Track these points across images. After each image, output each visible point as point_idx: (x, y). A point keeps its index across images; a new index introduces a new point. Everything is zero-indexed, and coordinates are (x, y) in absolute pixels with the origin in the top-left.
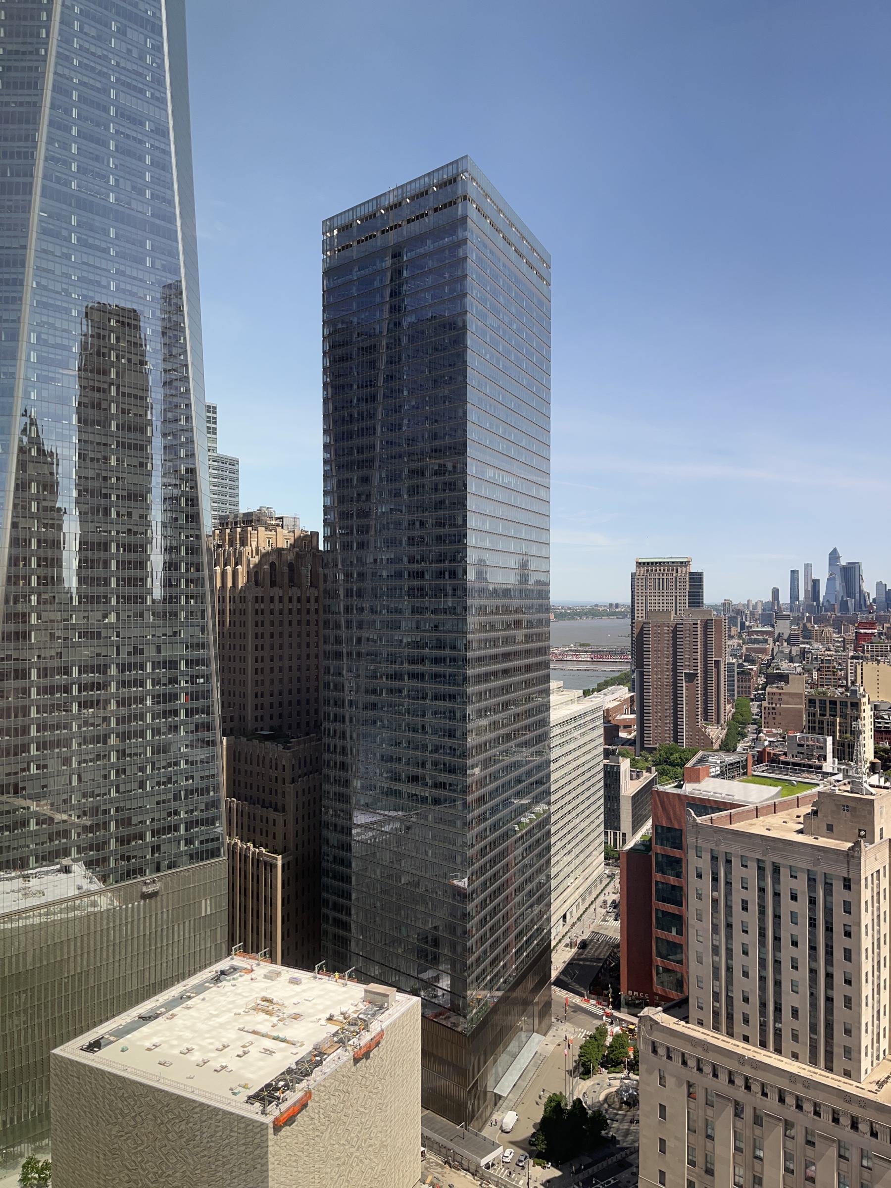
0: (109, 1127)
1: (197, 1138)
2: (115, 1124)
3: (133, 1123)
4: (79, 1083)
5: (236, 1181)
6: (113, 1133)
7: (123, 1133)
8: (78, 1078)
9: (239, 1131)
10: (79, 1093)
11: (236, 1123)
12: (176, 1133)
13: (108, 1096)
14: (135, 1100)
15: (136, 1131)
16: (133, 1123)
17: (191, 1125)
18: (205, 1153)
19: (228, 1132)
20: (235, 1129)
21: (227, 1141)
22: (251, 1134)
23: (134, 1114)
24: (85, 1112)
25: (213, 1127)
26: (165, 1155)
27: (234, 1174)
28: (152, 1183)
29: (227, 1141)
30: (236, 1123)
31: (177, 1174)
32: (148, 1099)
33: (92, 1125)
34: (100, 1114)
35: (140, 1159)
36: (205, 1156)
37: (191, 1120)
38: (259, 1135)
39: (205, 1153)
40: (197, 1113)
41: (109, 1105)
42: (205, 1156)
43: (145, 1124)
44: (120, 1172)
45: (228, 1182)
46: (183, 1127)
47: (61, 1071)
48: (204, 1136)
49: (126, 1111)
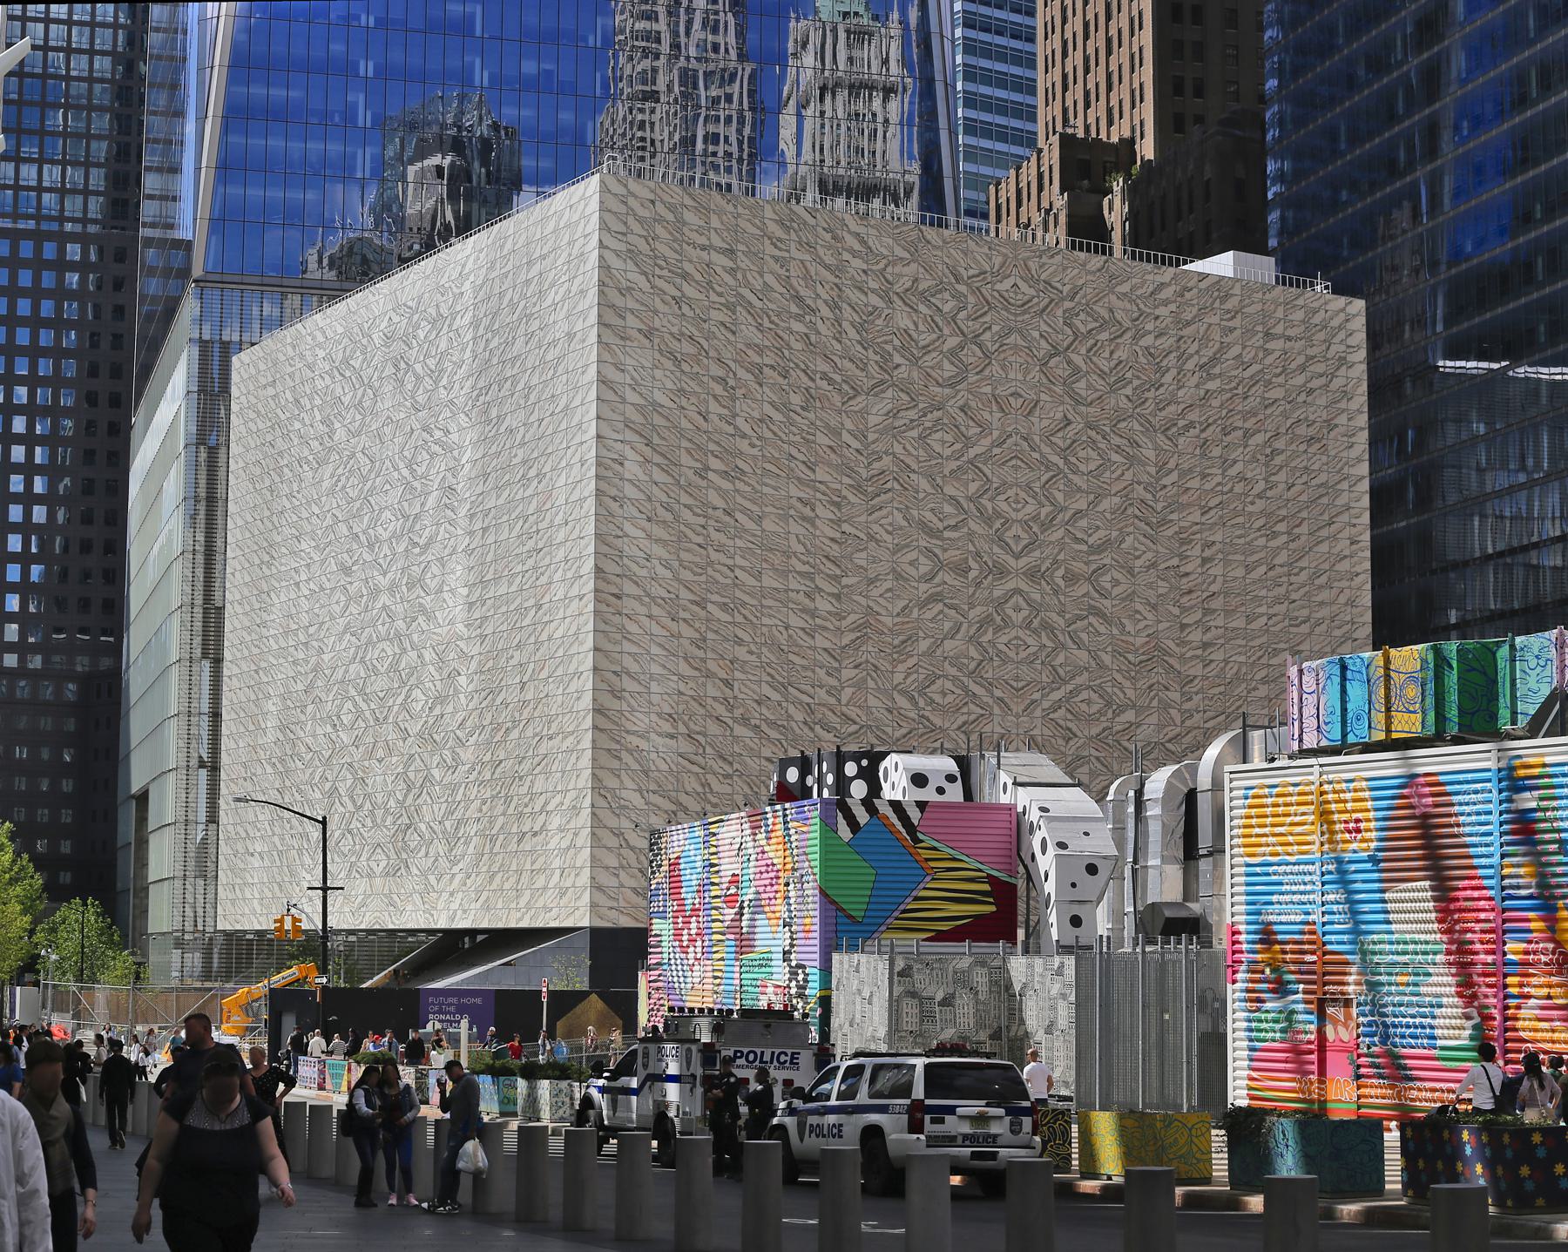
0: (859, 403)
1: (1168, 378)
2: (878, 388)
3: (949, 369)
4: (732, 272)
5: (1282, 477)
6: (873, 420)
7: (912, 414)
8: (730, 252)
9: (1290, 332)
10: (731, 308)
11: (1280, 314)
12: (1102, 375)
13: (855, 296)
14: (957, 296)
15: (962, 397)
16: (949, 369)
17: (1148, 340)
18: (1193, 416)
19: (1257, 340)
20: (1279, 329)
21: (1256, 368)
22: (1321, 336)
23: (952, 342)
24: (757, 371)
25: (1216, 335)
26: (1064, 452)
27: (1278, 460)
28: (1017, 557)
29: (1256, 368)
30: (1280, 314)
31: (1105, 504)
32: (1007, 284)
33: (785, 407)
34: (823, 366)
35: (973, 487)
36: (1191, 425)
37: (1149, 327)
38: (1342, 335)
39: (1193, 416)
40: (1166, 303)
41: (860, 328)
42: (1191, 425)
43: (996, 368)
44: (898, 549)
45: (1261, 485)
46: (1122, 354)
47: (651, 238)
48: (1190, 365)
49: (925, 338)
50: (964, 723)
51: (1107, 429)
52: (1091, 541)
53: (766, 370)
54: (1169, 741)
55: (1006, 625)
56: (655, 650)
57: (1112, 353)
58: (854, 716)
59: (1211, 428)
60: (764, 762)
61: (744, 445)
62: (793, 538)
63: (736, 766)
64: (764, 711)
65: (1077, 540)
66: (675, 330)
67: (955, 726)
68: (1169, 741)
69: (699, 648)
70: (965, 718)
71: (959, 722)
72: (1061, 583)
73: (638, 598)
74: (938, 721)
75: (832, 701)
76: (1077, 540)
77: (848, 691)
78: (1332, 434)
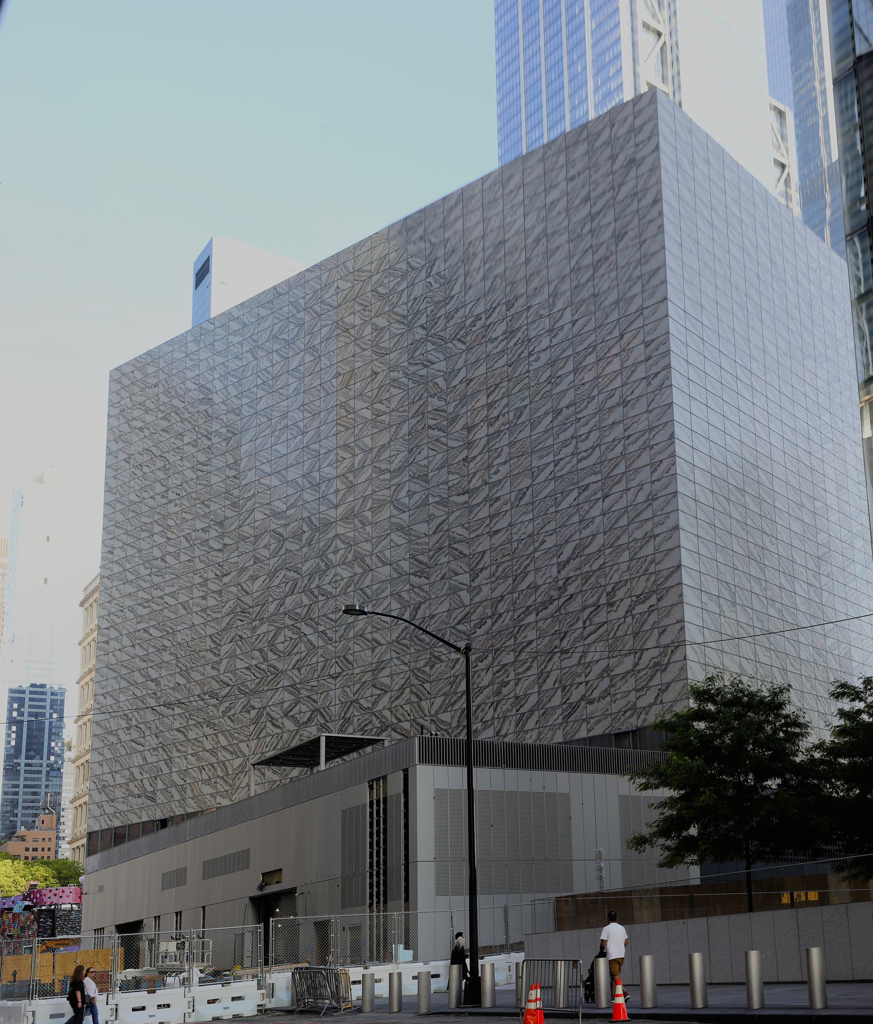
50: (297, 662)
51: (406, 364)
52: (393, 467)
53: (186, 448)
54: (458, 623)
55: (328, 569)
56: (124, 671)
57: (409, 296)
58: (227, 680)
59: (497, 310)
60: (176, 733)
61: (172, 508)
62: (197, 560)
63: (160, 739)
64: (177, 695)
65: (382, 472)
66: (140, 449)
67: (291, 667)
68: (458, 623)
69: (144, 661)
70: (297, 657)
71: (294, 662)
72: (368, 514)
73: (116, 639)
74: (280, 666)
75: (215, 673)
76: (382, 472)
77: (225, 662)
78: (621, 245)
